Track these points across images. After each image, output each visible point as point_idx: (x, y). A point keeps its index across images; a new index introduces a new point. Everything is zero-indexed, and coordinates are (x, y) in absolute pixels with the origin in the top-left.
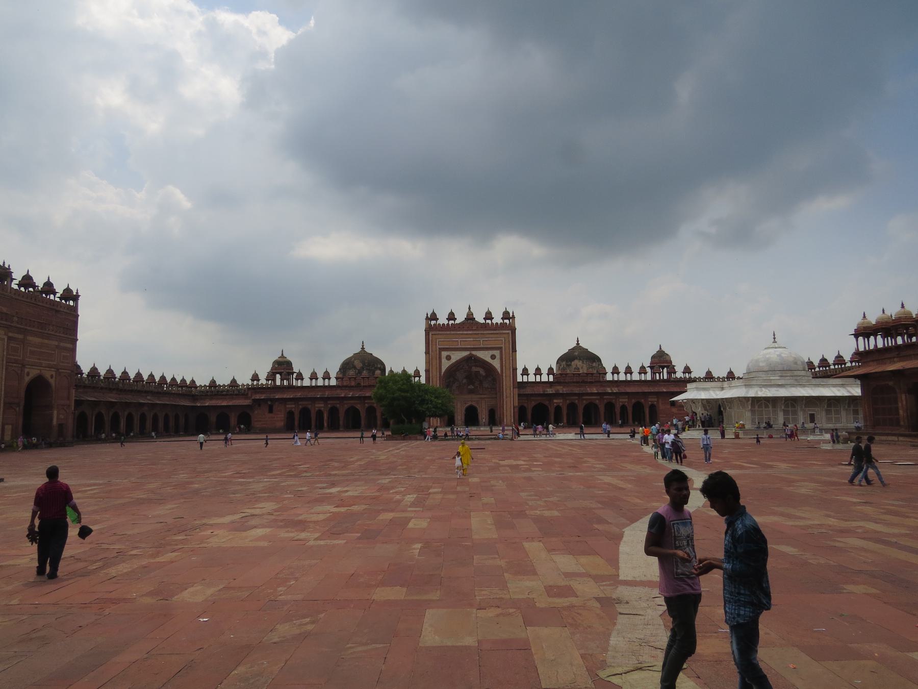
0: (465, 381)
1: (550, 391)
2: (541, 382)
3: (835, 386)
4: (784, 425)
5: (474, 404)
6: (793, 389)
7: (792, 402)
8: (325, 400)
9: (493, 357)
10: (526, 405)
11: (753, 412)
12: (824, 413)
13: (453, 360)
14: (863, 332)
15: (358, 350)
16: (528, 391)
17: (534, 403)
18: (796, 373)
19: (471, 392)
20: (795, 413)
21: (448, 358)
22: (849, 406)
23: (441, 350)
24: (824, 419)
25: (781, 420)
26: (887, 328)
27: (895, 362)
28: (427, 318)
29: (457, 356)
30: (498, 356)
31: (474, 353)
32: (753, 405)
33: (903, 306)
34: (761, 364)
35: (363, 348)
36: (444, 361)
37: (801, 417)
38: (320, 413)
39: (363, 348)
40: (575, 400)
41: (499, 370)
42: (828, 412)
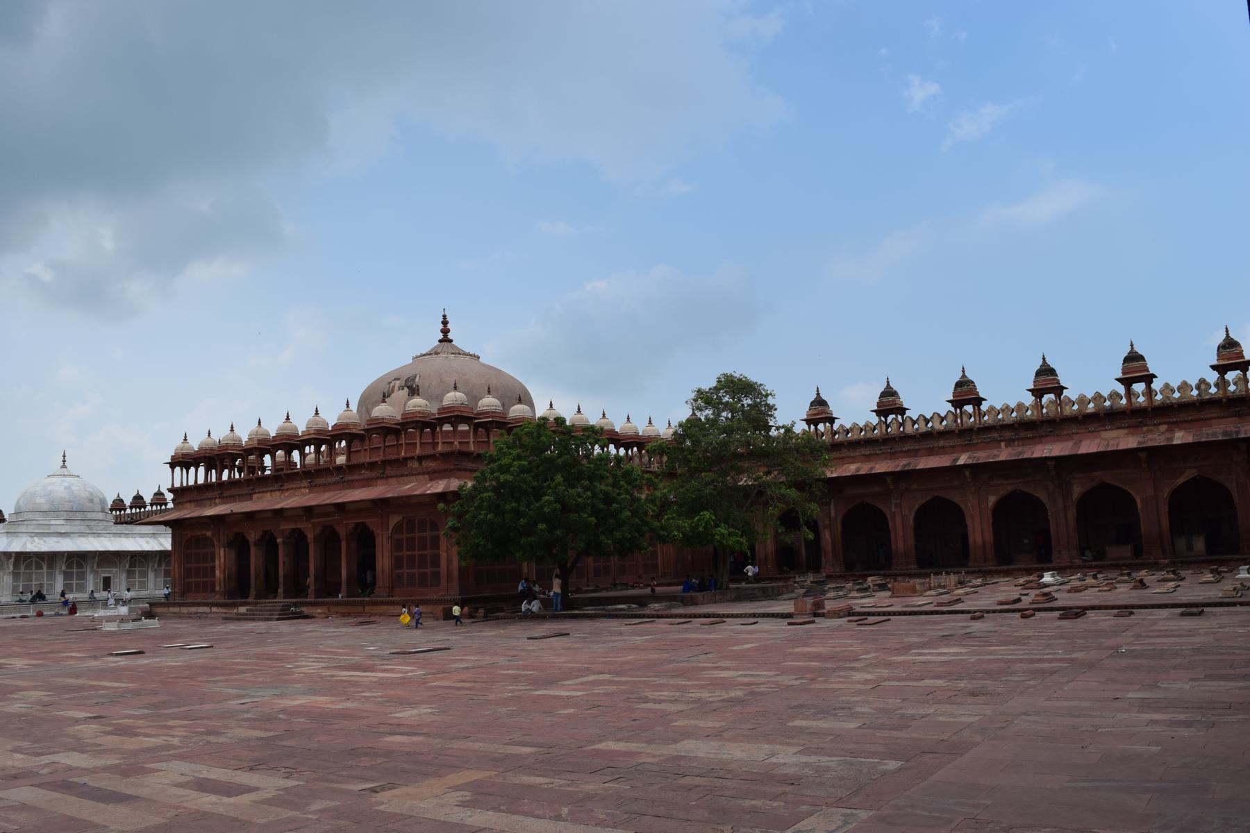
3: (142, 535)
4: (63, 594)
6: (83, 539)
7: (78, 560)
11: (16, 575)
12: (124, 576)
14: (182, 461)
18: (89, 516)
20: (82, 576)
22: (160, 565)
24: (124, 585)
25: (59, 586)
26: (214, 457)
27: (216, 505)
32: (16, 565)
33: (232, 430)
34: (39, 500)
37: (91, 582)
42: (130, 574)
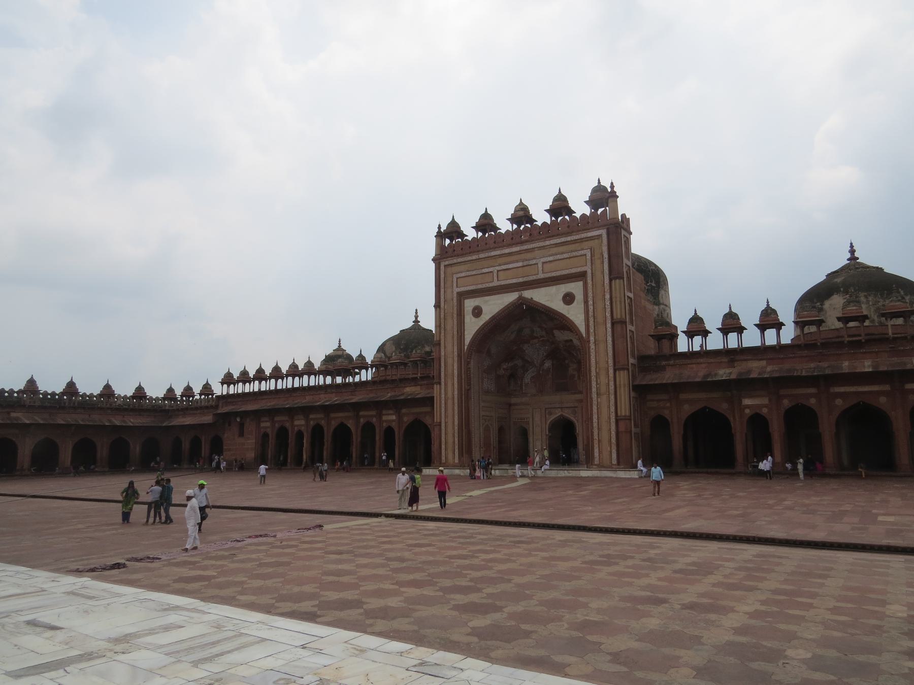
0: (548, 364)
1: (723, 373)
2: (705, 354)
5: (568, 414)
8: (306, 410)
9: (569, 299)
10: (666, 413)
13: (486, 317)
15: (409, 324)
16: (669, 376)
17: (688, 409)
19: (562, 388)
21: (477, 312)
23: (463, 296)
28: (440, 235)
29: (493, 306)
30: (579, 297)
31: (528, 294)
35: (416, 321)
36: (469, 318)
38: (300, 435)
39: (416, 321)
40: (810, 397)
41: (582, 329)
